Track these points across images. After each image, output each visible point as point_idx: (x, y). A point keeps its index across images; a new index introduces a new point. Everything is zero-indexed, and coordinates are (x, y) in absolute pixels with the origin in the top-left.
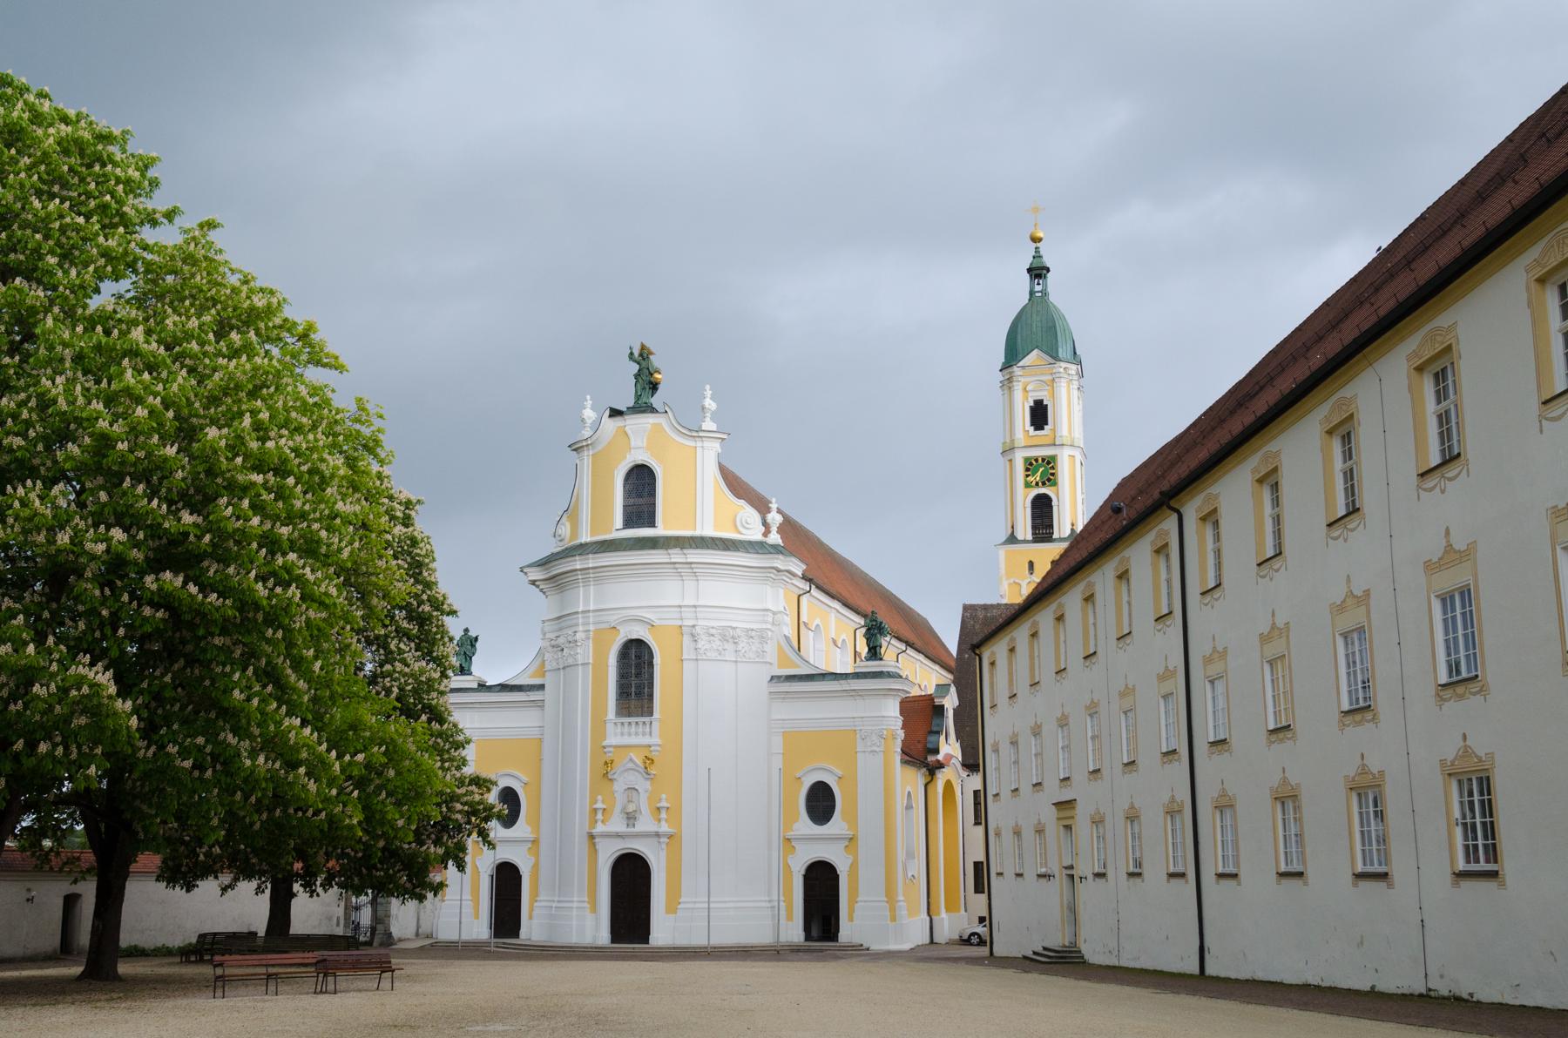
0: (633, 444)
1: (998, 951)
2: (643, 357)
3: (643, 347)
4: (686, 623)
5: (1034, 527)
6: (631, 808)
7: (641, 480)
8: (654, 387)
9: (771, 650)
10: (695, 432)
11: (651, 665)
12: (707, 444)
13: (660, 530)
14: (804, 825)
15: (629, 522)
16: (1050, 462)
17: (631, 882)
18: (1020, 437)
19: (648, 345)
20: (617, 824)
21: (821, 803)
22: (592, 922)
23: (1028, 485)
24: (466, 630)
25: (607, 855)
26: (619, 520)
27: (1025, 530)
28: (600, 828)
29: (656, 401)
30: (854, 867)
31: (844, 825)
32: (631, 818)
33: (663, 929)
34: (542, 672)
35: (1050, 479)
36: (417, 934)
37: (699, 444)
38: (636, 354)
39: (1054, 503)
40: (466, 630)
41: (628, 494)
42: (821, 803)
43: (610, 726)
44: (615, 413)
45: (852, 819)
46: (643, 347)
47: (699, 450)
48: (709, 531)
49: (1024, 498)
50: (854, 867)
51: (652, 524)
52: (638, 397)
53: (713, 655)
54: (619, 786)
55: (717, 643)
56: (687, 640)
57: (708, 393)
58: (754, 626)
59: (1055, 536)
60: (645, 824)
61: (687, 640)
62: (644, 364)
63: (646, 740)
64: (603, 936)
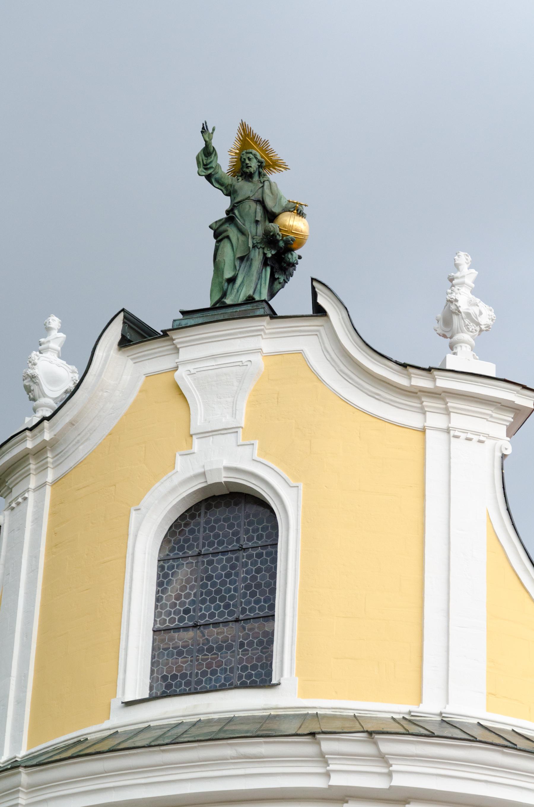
0: (199, 420)
2: (244, 173)
3: (247, 139)
10: (416, 380)
12: (464, 419)
13: (289, 694)
19: (261, 131)
26: (136, 677)
37: (435, 420)
38: (224, 162)
46: (247, 139)
47: (435, 441)
48: (471, 707)
52: (224, 284)
57: (468, 274)
62: (246, 189)
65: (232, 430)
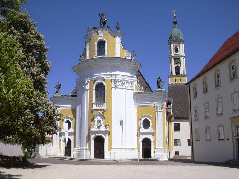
1: (195, 160)
4: (113, 79)
5: (176, 72)
6: (99, 124)
7: (102, 44)
8: (105, 23)
9: (134, 88)
11: (104, 89)
14: (143, 130)
15: (98, 54)
16: (179, 59)
17: (99, 143)
18: (173, 55)
20: (94, 129)
21: (146, 124)
22: (89, 153)
23: (175, 64)
24: (58, 83)
25: (92, 136)
26: (96, 53)
27: (174, 73)
28: (91, 129)
29: (106, 26)
30: (155, 140)
31: (153, 130)
32: (99, 127)
33: (108, 155)
34: (76, 93)
35: (179, 63)
36: (46, 155)
39: (180, 67)
40: (58, 83)
41: (98, 48)
42: (146, 124)
43: (94, 105)
44: (95, 28)
45: (154, 127)
49: (174, 67)
50: (155, 140)
51: (104, 54)
53: (120, 87)
54: (96, 120)
55: (121, 84)
56: (113, 83)
58: (130, 80)
59: (180, 74)
60: (103, 129)
61: (113, 83)
63: (103, 108)
64: (92, 157)
65: (102, 37)
